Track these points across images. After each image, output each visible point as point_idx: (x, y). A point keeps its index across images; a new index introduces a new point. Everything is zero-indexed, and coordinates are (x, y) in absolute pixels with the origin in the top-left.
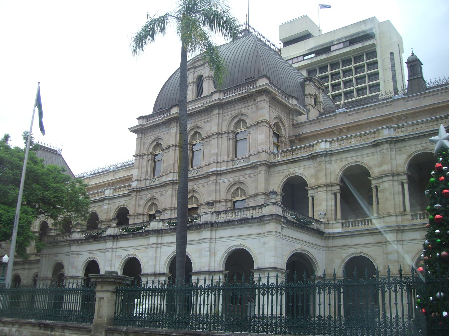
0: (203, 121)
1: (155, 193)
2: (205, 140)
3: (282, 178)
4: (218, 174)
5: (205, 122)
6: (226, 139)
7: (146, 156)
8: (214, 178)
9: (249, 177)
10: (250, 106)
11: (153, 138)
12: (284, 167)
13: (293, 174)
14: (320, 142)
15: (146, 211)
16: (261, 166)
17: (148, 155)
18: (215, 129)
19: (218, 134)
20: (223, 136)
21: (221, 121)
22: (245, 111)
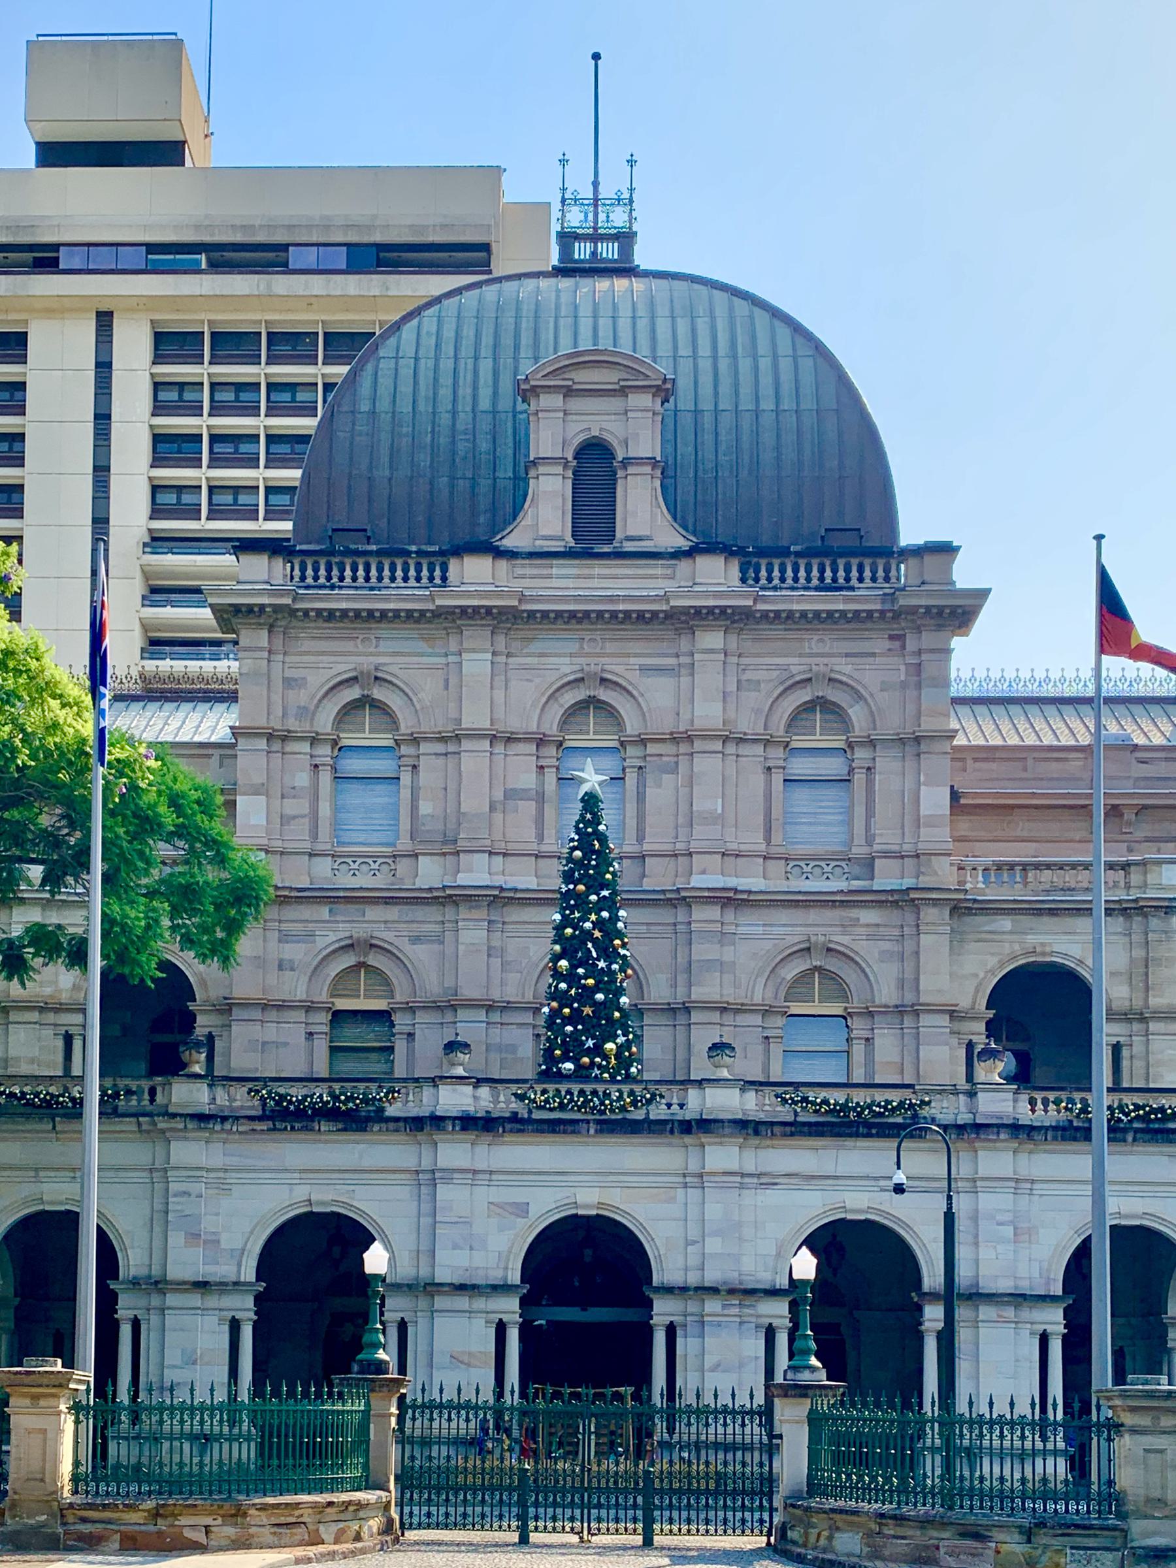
0: (632, 660)
1: (373, 922)
2: (651, 749)
3: (992, 961)
4: (731, 900)
5: (643, 669)
6: (760, 769)
7: (305, 747)
8: (714, 912)
9: (870, 938)
10: (873, 655)
11: (344, 667)
12: (1006, 923)
13: (1044, 954)
14: (1160, 862)
15: (322, 995)
16: (934, 905)
17: (314, 741)
18: (708, 713)
19: (726, 740)
20: (745, 749)
21: (733, 687)
22: (848, 669)
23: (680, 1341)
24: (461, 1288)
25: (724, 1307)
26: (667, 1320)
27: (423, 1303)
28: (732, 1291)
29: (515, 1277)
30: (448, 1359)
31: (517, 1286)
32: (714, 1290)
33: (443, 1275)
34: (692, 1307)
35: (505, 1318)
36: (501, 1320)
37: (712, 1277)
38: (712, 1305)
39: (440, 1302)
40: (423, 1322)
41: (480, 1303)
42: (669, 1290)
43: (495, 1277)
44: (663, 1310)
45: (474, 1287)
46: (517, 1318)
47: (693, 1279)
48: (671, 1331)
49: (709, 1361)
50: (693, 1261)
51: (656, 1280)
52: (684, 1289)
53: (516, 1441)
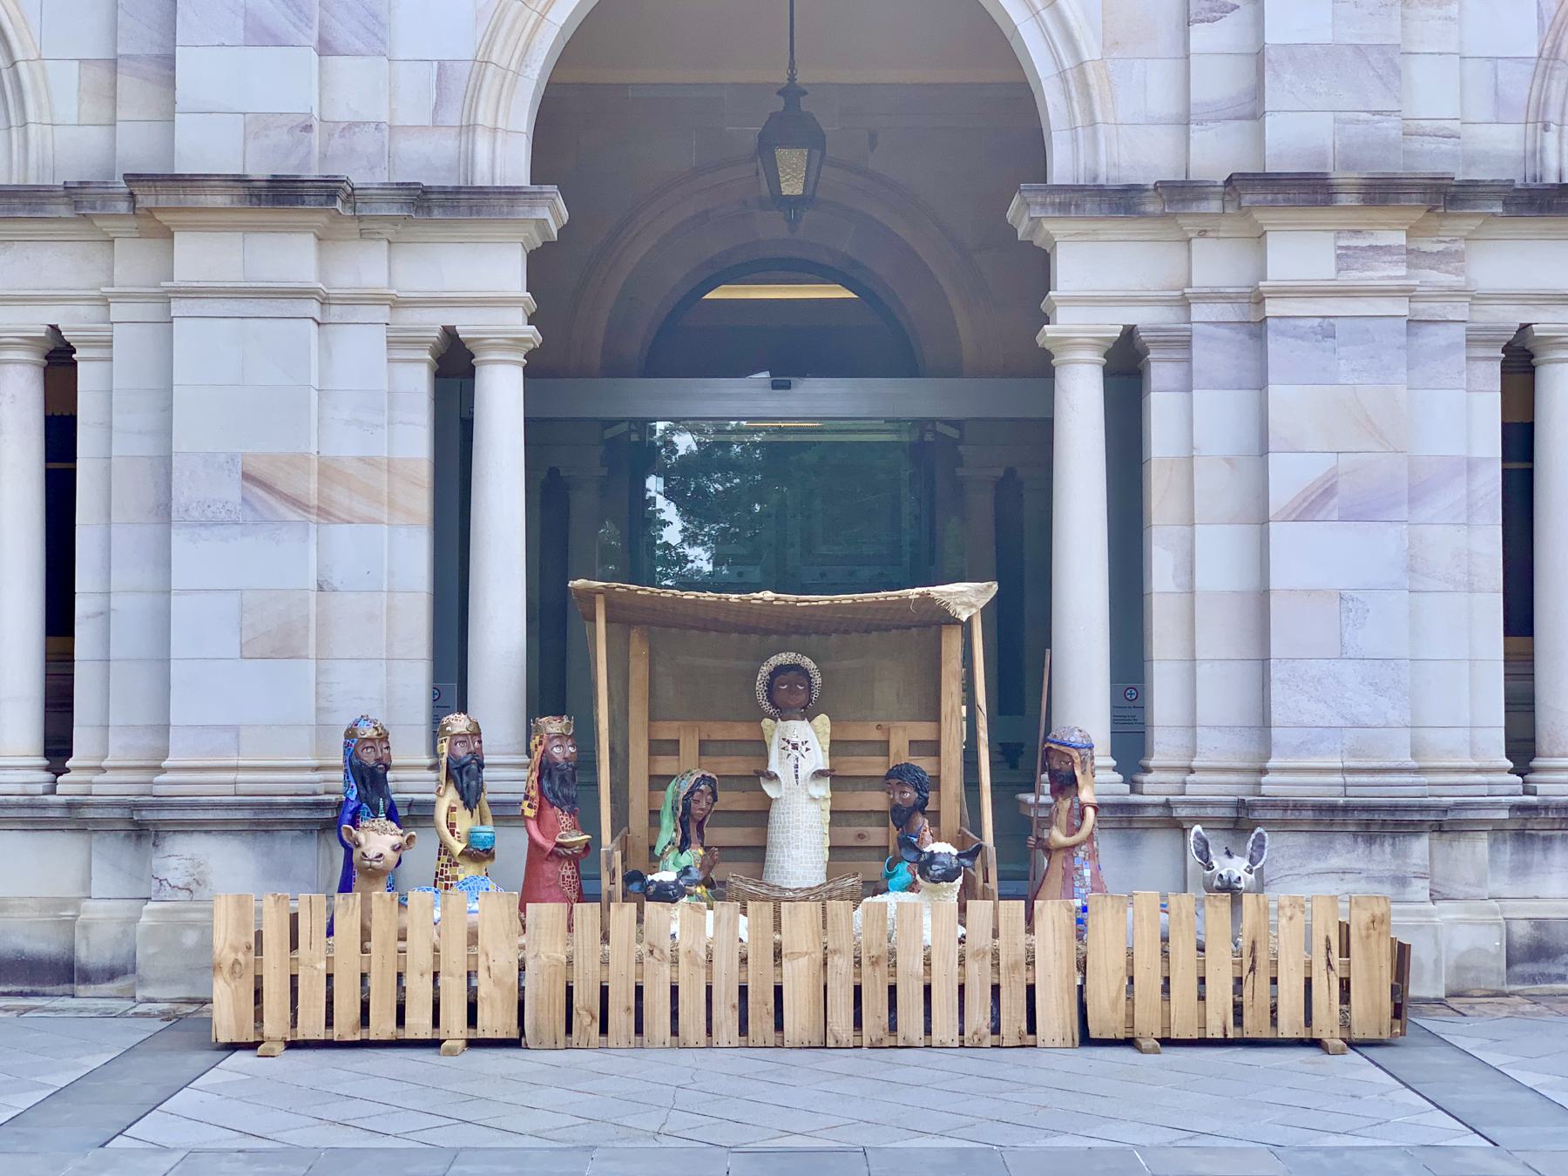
23: (1162, 407)
24: (279, 195)
25: (1345, 257)
26: (1112, 322)
27: (131, 263)
28: (1382, 192)
29: (506, 157)
30: (231, 491)
31: (512, 193)
32: (1308, 190)
33: (207, 146)
34: (1215, 264)
35: (467, 323)
36: (450, 333)
37: (1296, 134)
38: (1300, 253)
39: (201, 256)
40: (131, 340)
41: (366, 266)
42: (1120, 201)
43: (426, 159)
44: (1096, 283)
45: (330, 190)
46: (515, 323)
47: (1215, 154)
48: (1126, 368)
49: (1290, 476)
50: (1216, 82)
51: (1065, 162)
52: (1180, 193)
53: (505, 814)
